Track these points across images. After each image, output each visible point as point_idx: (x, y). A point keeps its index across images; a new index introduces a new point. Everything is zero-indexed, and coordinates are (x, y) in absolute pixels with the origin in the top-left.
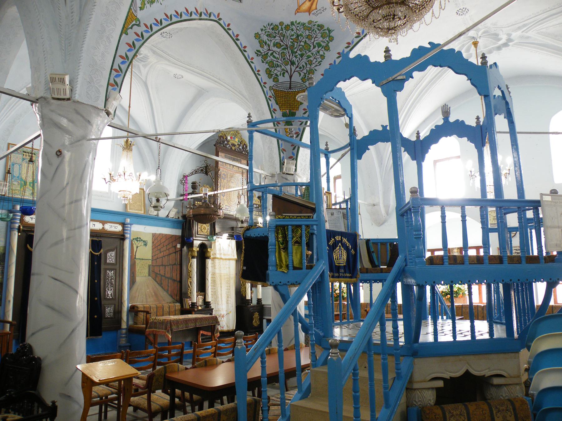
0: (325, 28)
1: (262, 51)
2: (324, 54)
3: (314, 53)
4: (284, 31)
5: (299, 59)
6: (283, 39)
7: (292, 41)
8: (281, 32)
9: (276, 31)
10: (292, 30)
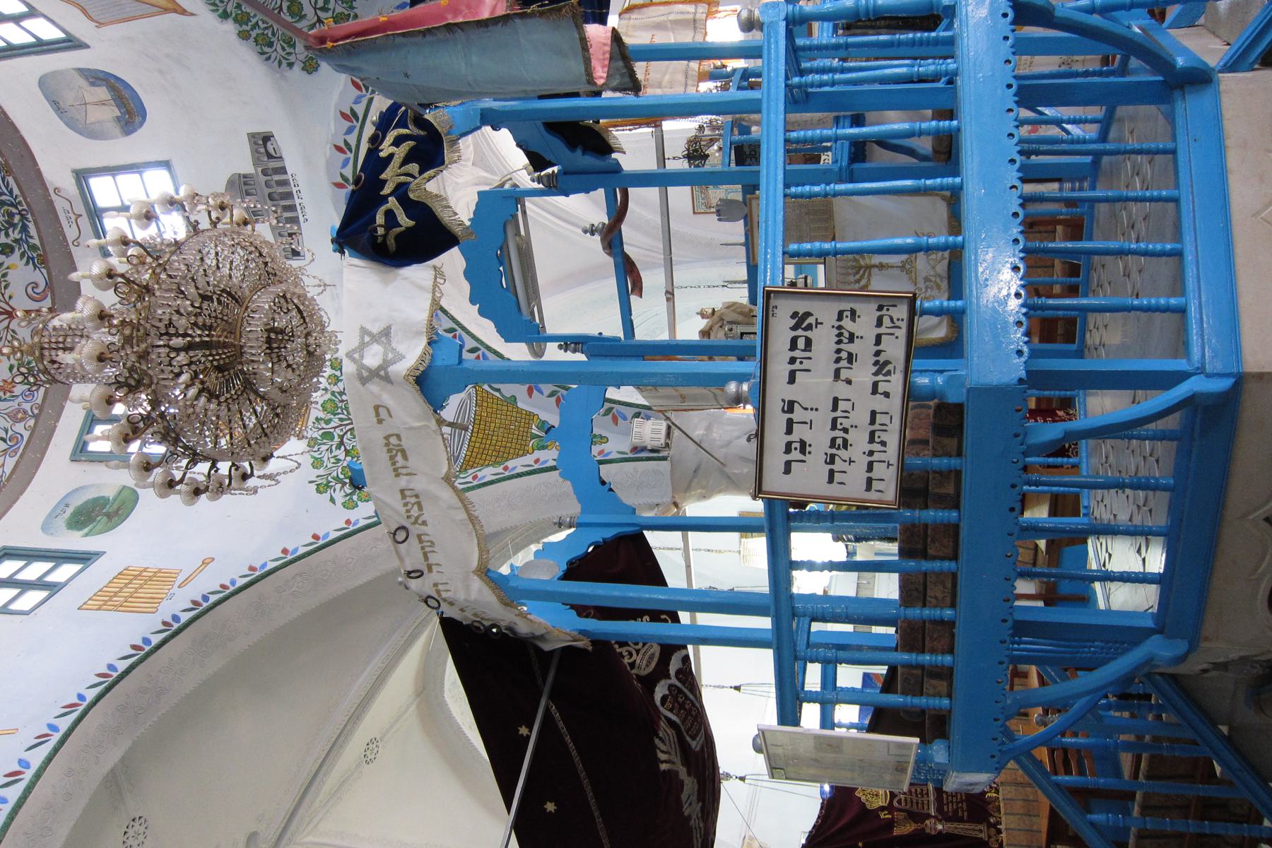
4: (254, 21)
8: (262, 26)
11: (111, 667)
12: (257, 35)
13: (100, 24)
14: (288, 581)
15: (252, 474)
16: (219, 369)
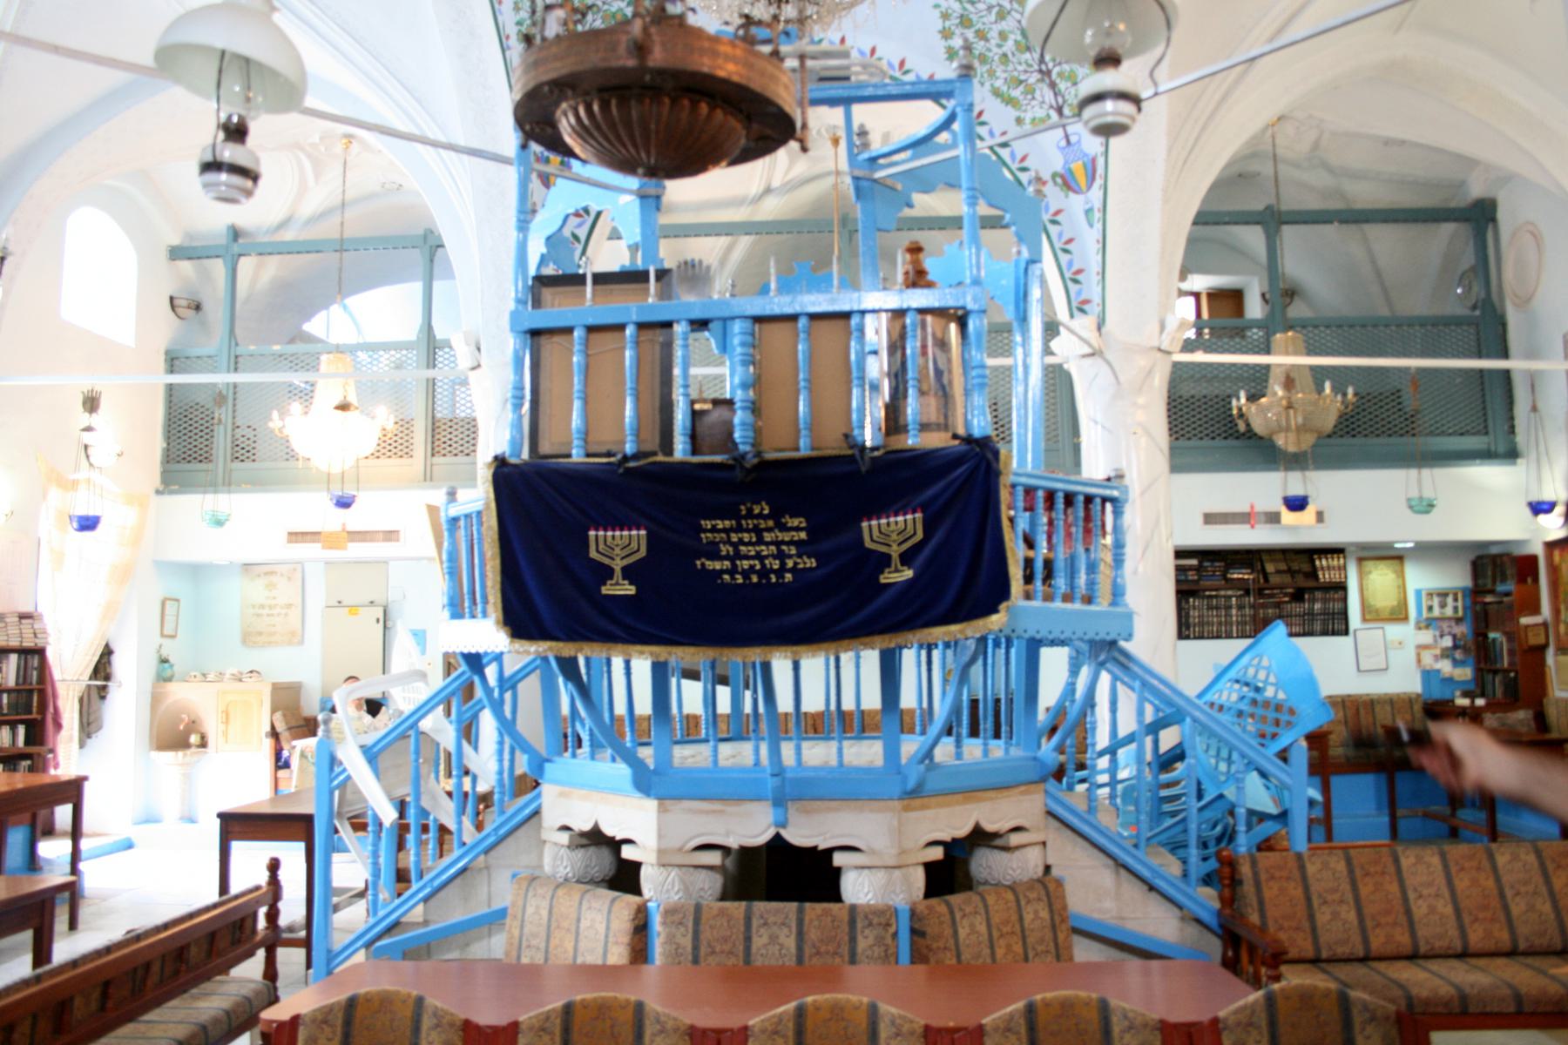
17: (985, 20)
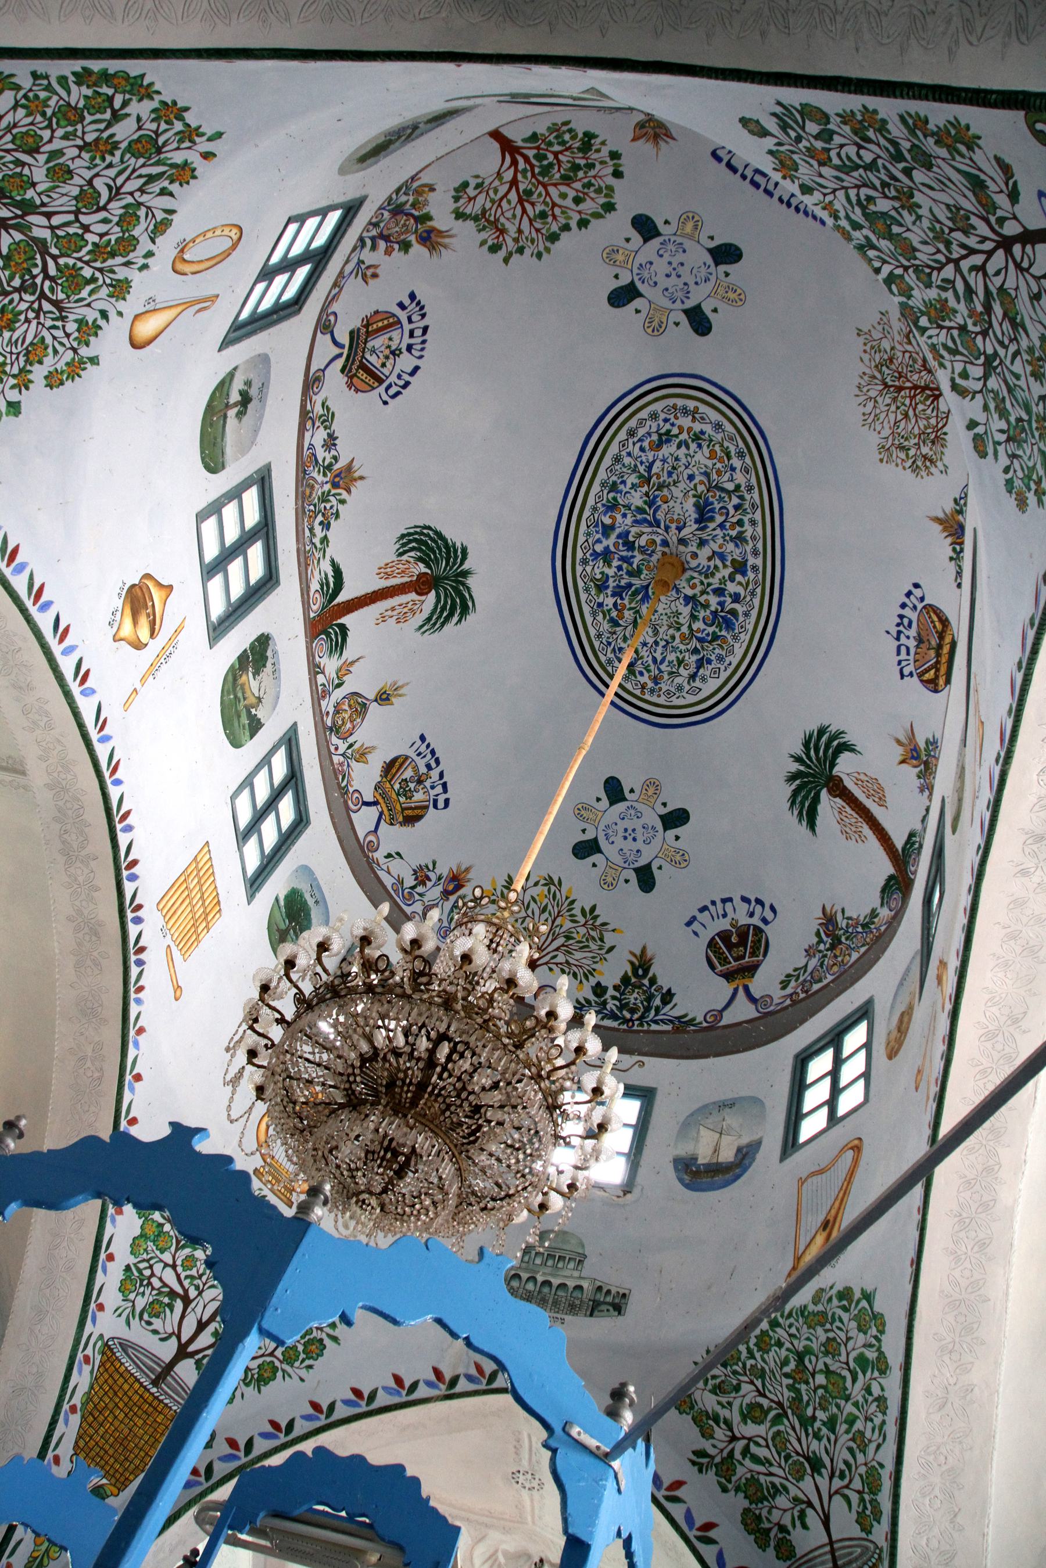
0: (858, 1294)
1: (712, 1451)
2: (883, 1389)
3: (861, 1400)
4: (758, 1355)
5: (829, 1440)
6: (764, 1385)
7: (790, 1381)
9: (735, 1367)
10: (779, 1344)
11: (129, 829)
12: (740, 1353)
13: (802, 1182)
14: (103, 1060)
15: (250, 1062)
16: (391, 1085)
17: (112, 172)
